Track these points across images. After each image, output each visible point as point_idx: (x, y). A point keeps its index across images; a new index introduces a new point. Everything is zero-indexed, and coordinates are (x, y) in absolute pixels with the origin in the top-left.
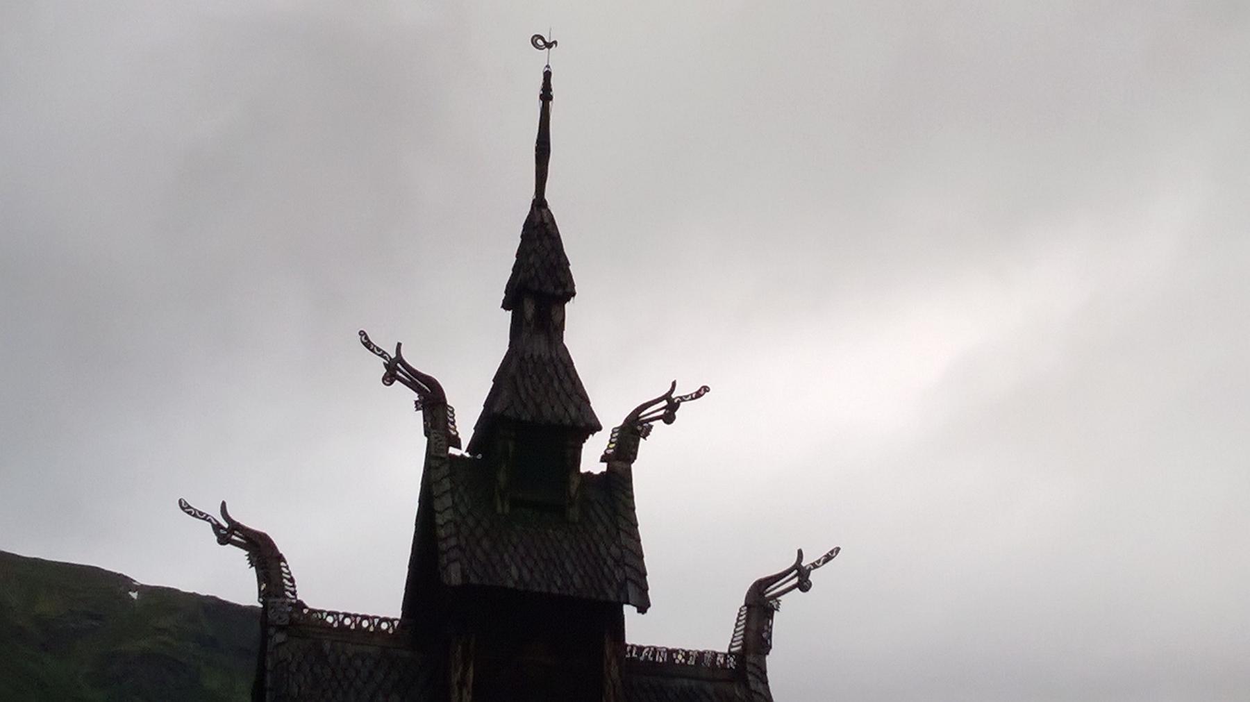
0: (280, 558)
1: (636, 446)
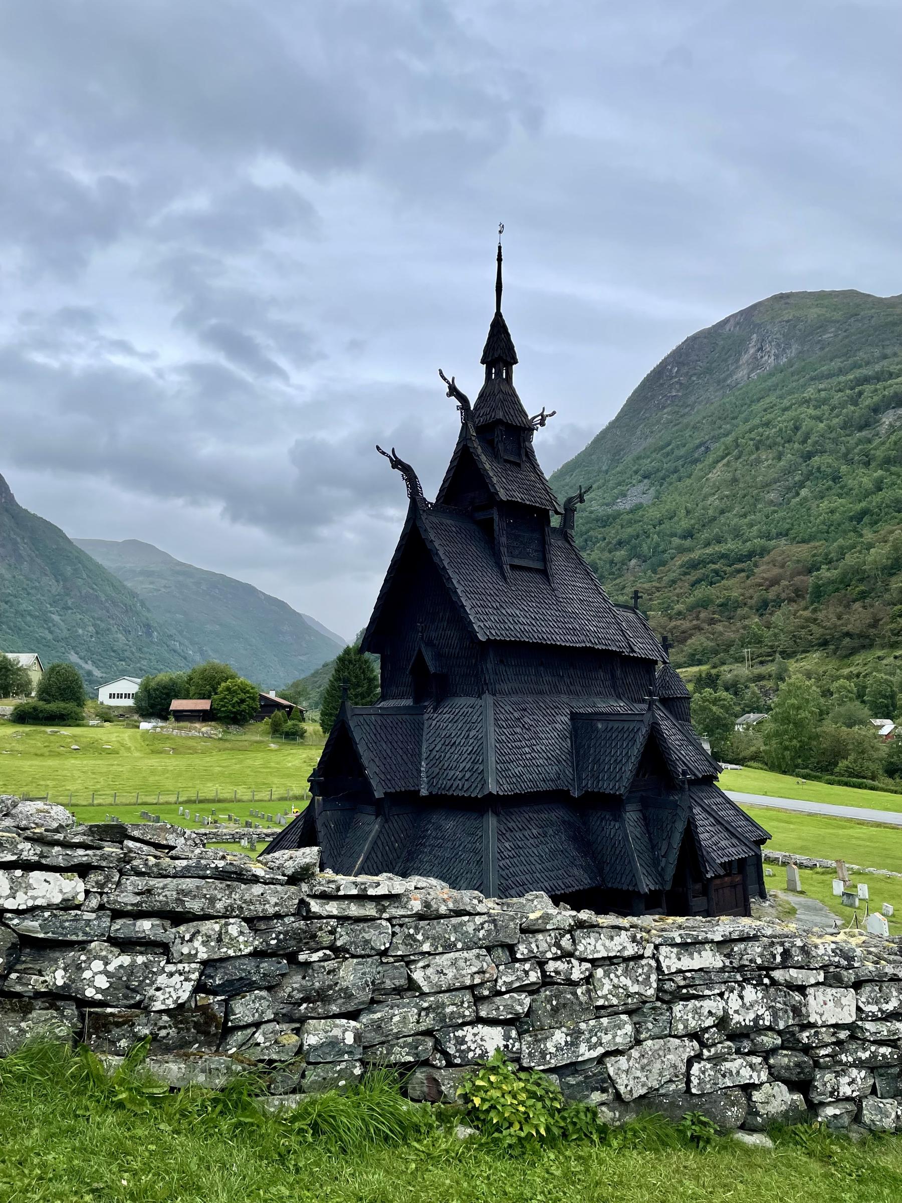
0: (416, 477)
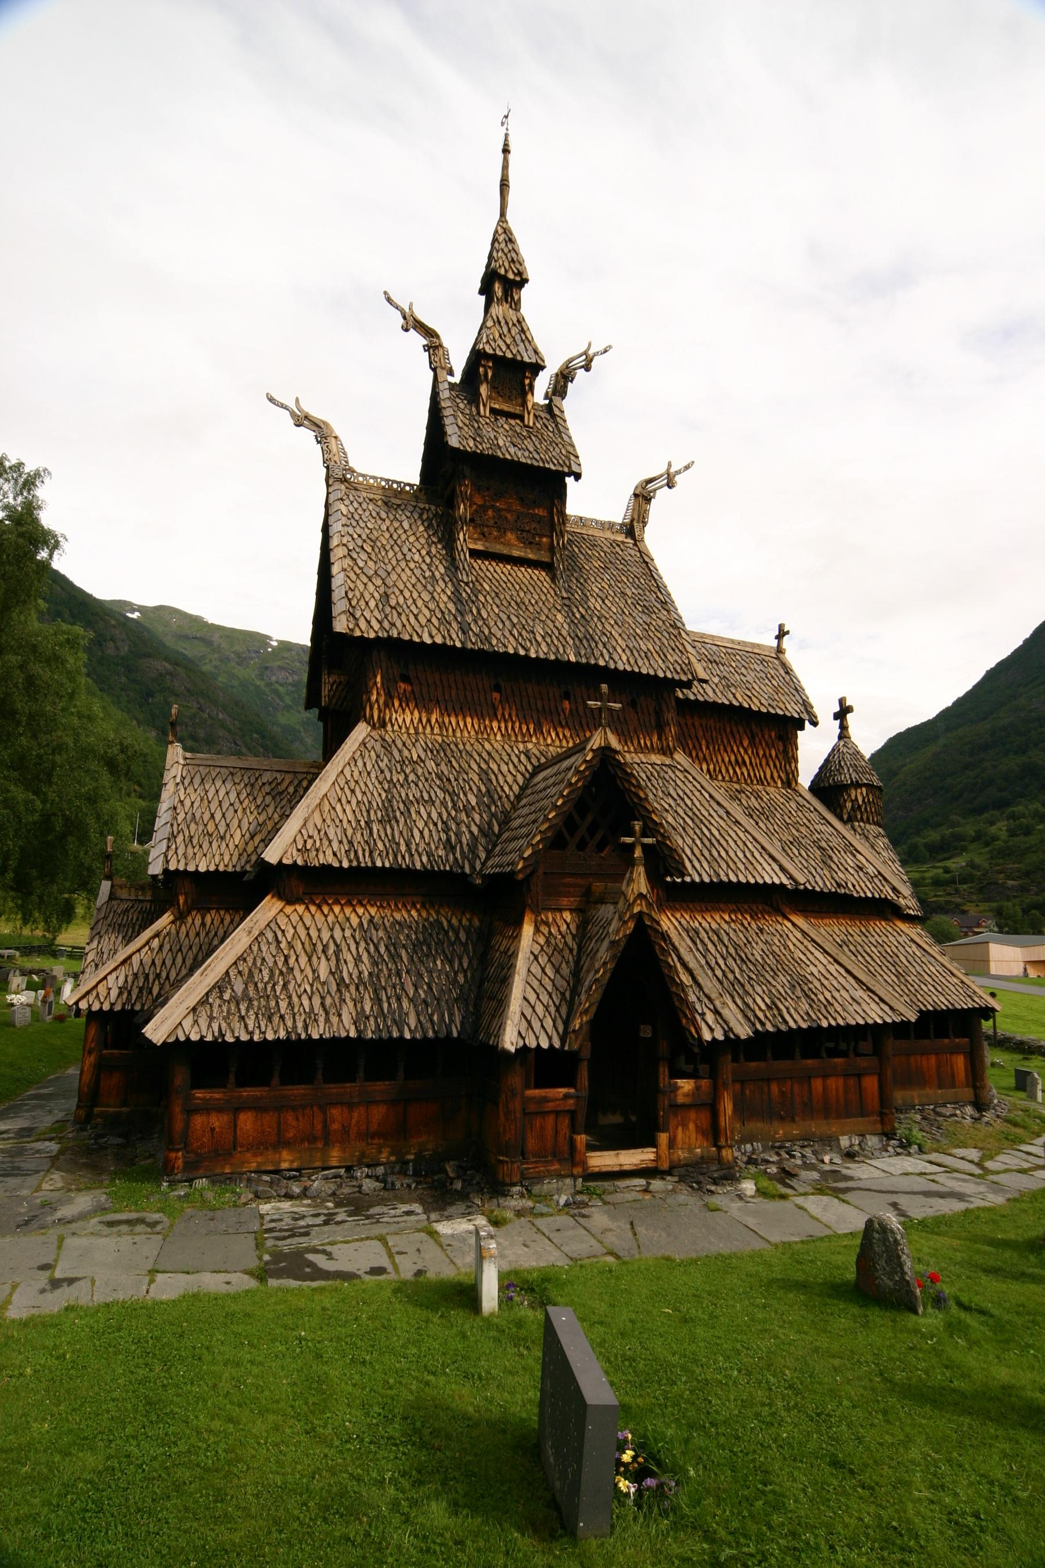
1: (566, 386)
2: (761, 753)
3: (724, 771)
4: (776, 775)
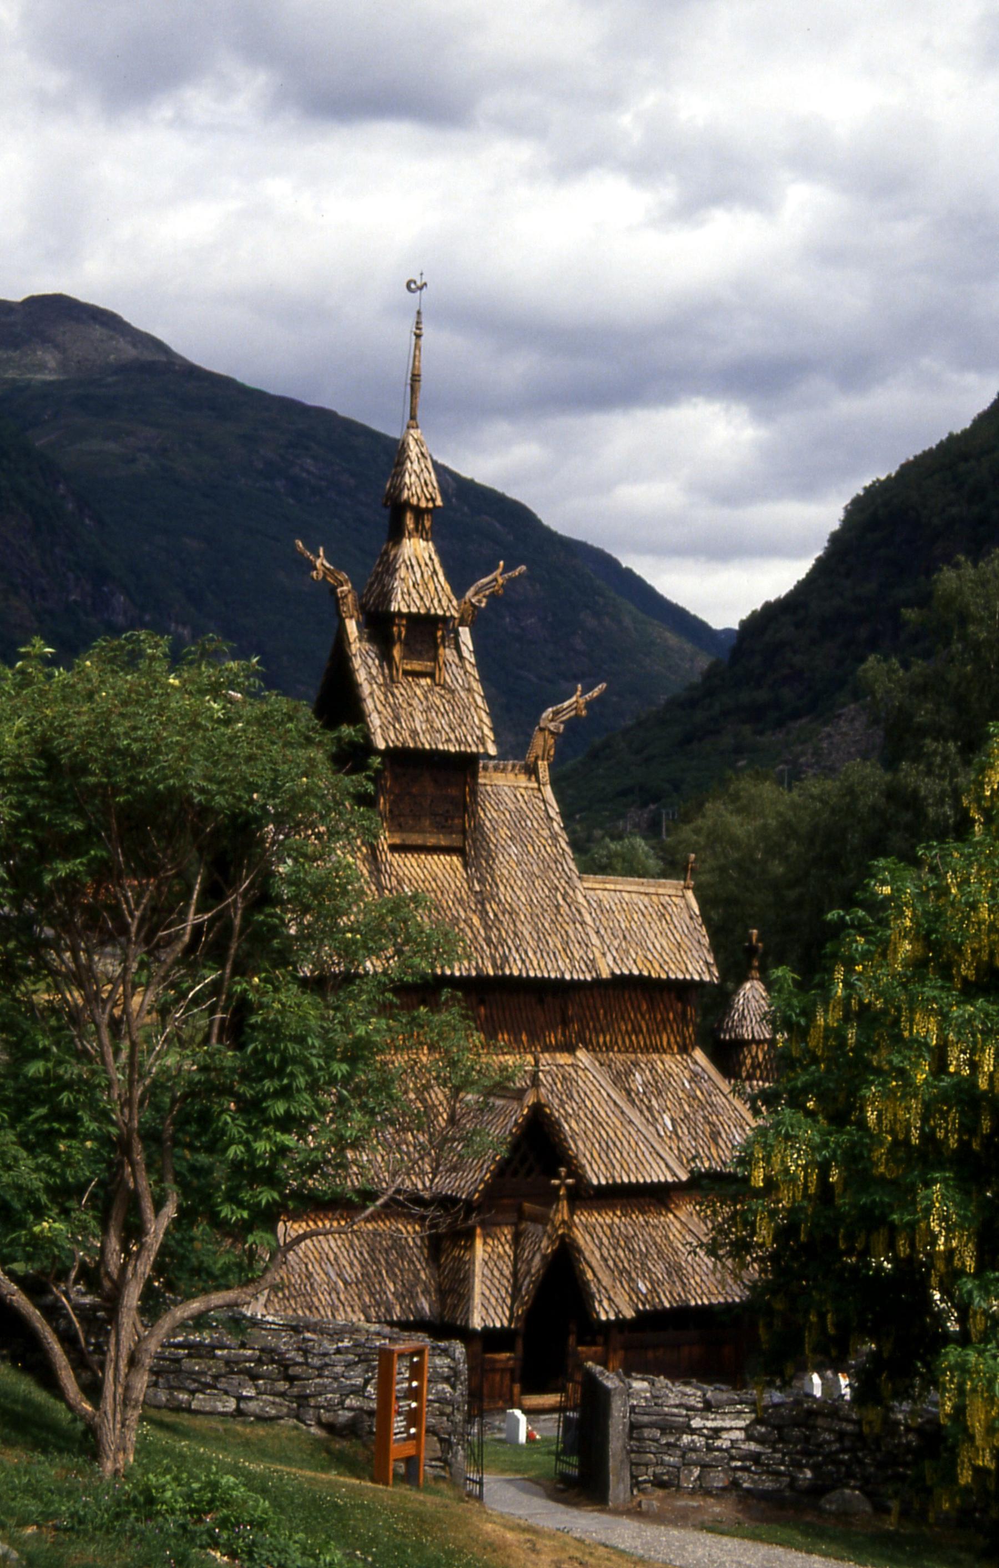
2: (659, 1017)
3: (620, 1042)
4: (672, 1040)
